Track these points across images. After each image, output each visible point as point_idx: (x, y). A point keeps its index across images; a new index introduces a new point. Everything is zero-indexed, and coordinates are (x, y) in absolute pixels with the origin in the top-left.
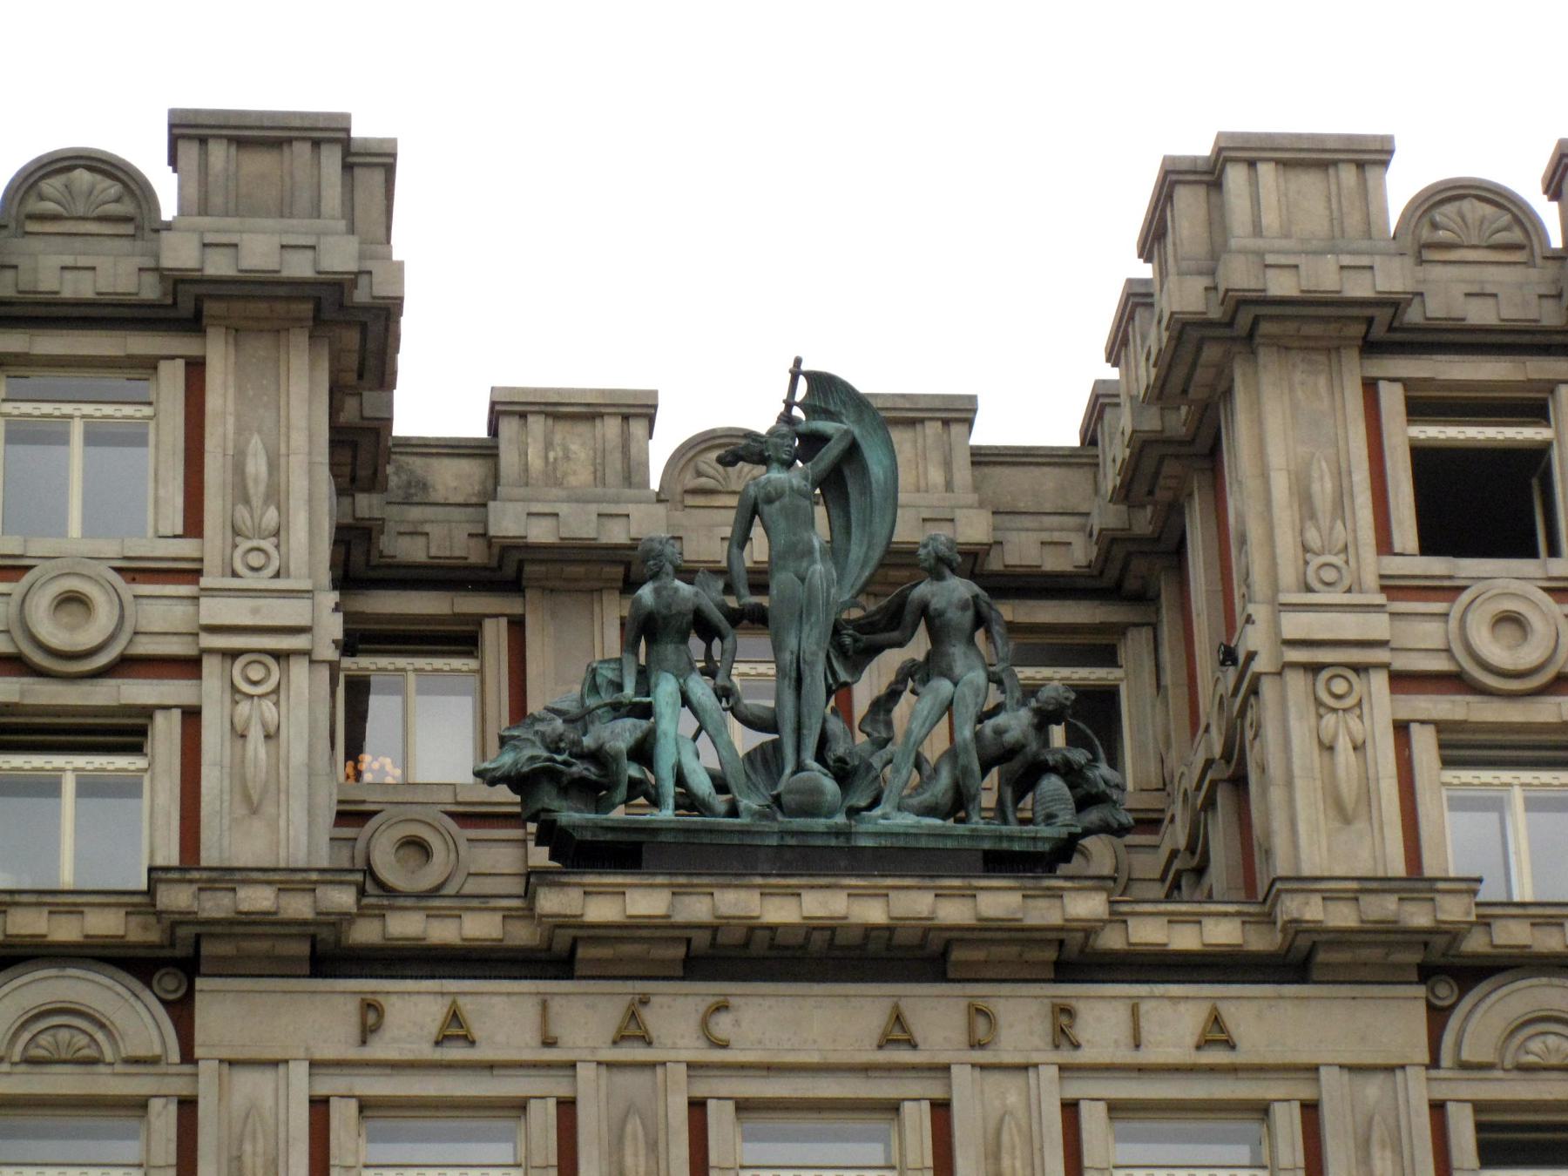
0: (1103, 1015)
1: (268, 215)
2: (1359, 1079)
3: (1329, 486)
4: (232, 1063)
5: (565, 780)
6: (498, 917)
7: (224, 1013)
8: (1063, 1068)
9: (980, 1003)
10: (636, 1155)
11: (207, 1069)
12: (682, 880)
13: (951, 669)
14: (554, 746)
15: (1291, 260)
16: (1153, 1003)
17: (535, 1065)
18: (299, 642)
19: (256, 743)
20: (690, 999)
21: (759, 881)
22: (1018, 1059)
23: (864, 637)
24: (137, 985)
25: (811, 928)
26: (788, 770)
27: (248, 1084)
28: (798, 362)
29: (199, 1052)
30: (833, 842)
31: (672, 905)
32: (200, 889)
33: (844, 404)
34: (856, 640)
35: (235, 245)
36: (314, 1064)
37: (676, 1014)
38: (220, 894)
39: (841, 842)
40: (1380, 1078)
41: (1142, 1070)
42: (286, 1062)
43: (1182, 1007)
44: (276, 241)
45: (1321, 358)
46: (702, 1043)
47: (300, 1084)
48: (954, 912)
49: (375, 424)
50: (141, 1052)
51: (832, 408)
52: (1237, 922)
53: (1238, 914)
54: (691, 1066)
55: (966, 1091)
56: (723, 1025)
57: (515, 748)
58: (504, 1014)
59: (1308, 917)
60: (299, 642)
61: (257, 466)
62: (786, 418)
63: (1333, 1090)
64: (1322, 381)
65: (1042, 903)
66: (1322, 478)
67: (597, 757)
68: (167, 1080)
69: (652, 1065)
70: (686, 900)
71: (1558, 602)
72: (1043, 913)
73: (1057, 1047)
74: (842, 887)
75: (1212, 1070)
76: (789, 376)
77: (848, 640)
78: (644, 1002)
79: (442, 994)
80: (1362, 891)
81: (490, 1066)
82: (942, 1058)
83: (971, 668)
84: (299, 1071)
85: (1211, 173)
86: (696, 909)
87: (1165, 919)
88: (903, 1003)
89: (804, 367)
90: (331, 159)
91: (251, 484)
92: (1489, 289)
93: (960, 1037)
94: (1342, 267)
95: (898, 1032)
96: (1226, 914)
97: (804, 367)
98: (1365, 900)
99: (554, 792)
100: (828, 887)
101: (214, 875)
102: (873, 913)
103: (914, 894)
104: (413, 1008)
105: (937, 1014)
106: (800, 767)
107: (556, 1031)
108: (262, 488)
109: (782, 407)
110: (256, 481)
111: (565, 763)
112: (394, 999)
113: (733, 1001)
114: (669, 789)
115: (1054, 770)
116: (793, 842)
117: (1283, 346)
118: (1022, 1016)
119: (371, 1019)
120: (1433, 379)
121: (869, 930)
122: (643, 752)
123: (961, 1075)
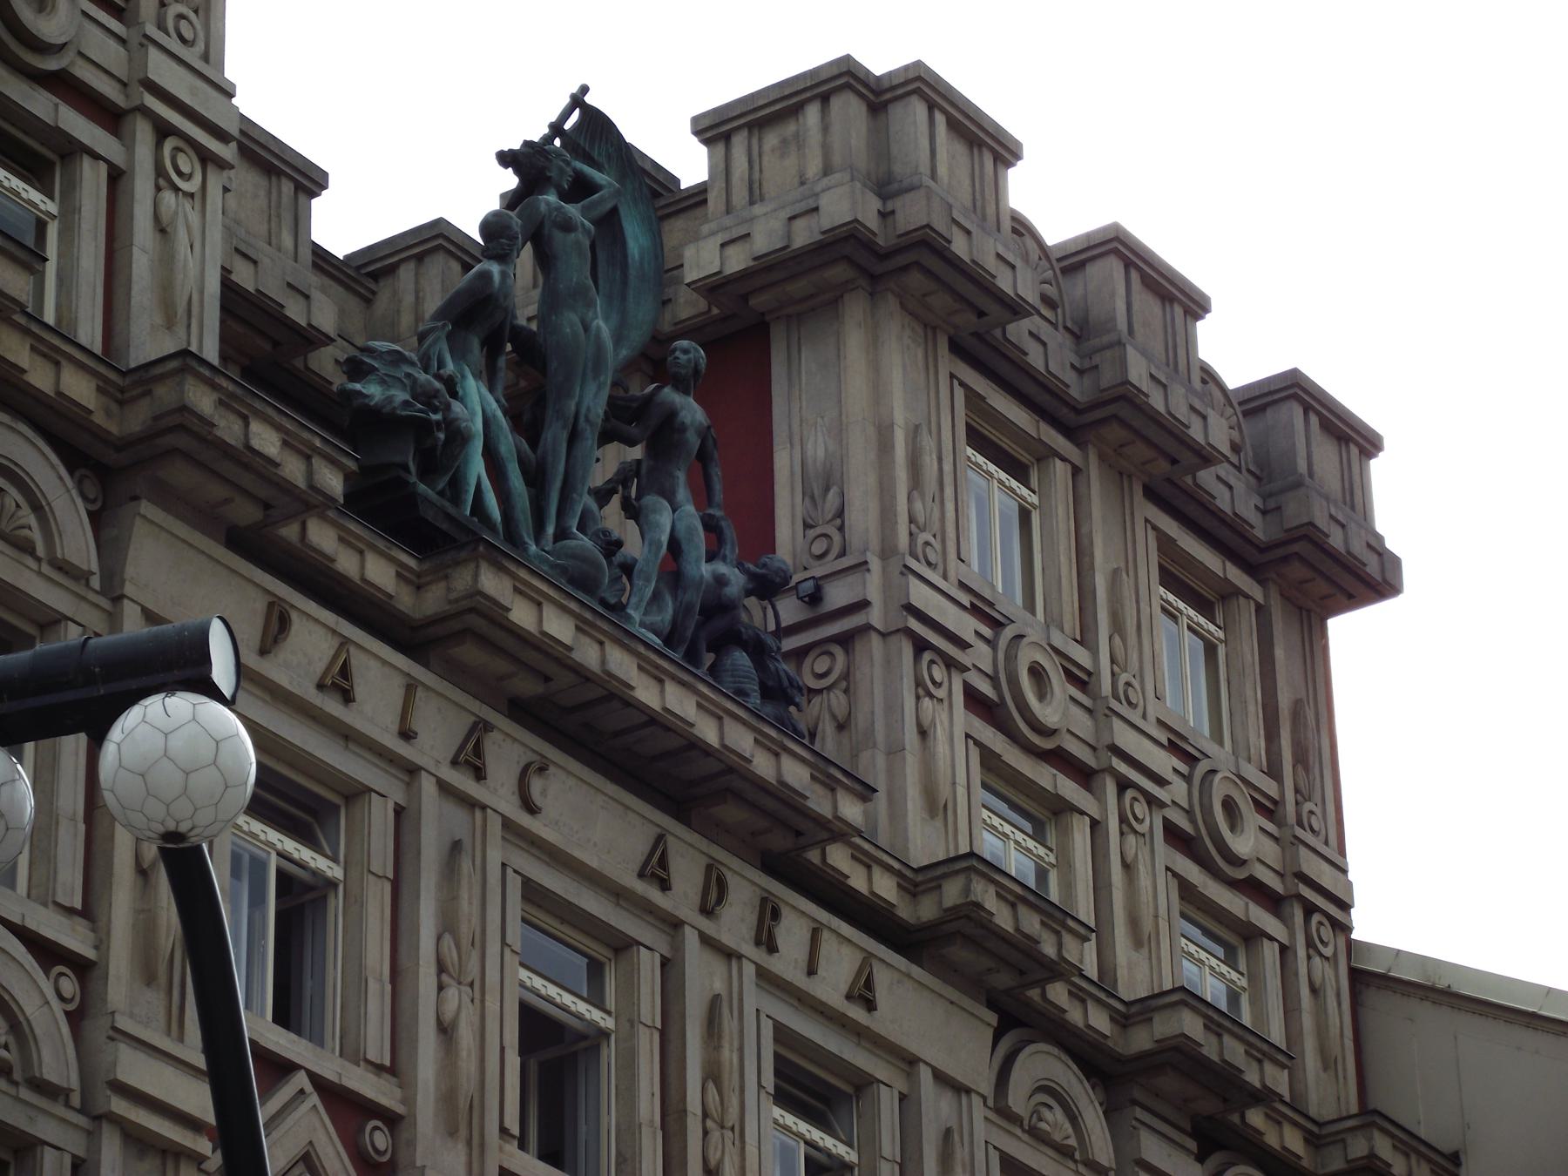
20: (516, 745)
25: (654, 721)
28: (584, 89)
33: (609, 157)
46: (515, 799)
51: (595, 155)
57: (382, 382)
62: (548, 139)
68: (84, 606)
76: (566, 100)
79: (334, 632)
81: (348, 736)
85: (877, 93)
86: (588, 654)
89: (588, 99)
95: (657, 870)
107: (416, 725)
115: (744, 645)
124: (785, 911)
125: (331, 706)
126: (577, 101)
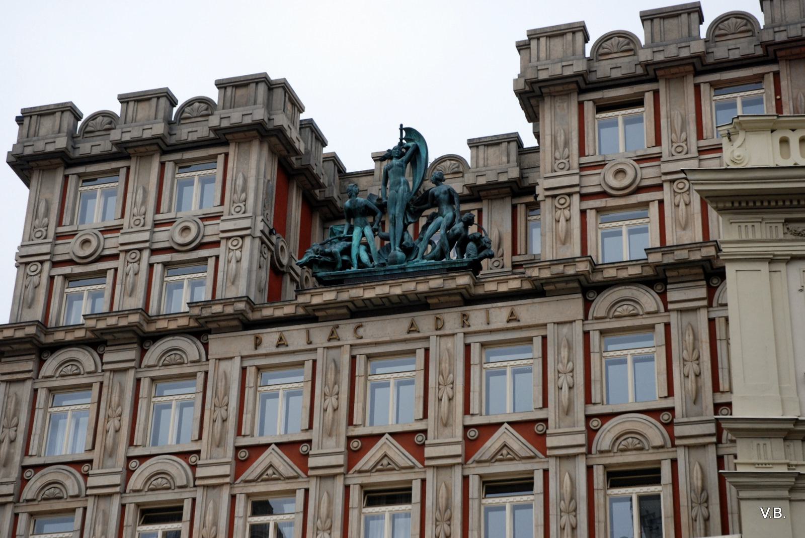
0: (477, 316)
1: (243, 106)
2: (560, 327)
3: (563, 137)
4: (220, 359)
5: (319, 263)
6: (294, 307)
7: (218, 345)
8: (465, 334)
9: (438, 316)
10: (331, 375)
11: (212, 362)
12: (339, 288)
13: (442, 213)
14: (316, 252)
15: (546, 67)
16: (493, 309)
17: (306, 350)
18: (248, 232)
19: (233, 264)
21: (362, 285)
22: (450, 332)
23: (417, 207)
24: (195, 339)
26: (392, 251)
27: (224, 365)
28: (401, 125)
29: (209, 357)
30: (400, 272)
31: (337, 296)
32: (202, 308)
34: (414, 208)
35: (229, 117)
36: (242, 357)
37: (346, 331)
38: (207, 309)
39: (403, 271)
40: (568, 325)
41: (491, 331)
42: (234, 357)
43: (503, 310)
44: (241, 113)
45: (566, 97)
47: (237, 364)
48: (422, 288)
49: (306, 167)
50: (194, 359)
51: (412, 138)
52: (520, 280)
53: (519, 278)
54: (351, 346)
55: (433, 344)
56: (361, 331)
58: (296, 336)
59: (533, 275)
60: (248, 232)
61: (240, 182)
63: (550, 331)
64: (565, 105)
65: (450, 281)
66: (561, 135)
67: (331, 254)
68: (203, 366)
69: (340, 347)
70: (342, 294)
71: (638, 164)
72: (451, 284)
73: (463, 327)
74: (387, 284)
75: (514, 329)
76: (399, 131)
77: (411, 209)
78: (337, 327)
80: (550, 265)
82: (427, 334)
83: (448, 212)
84: (237, 360)
86: (345, 296)
87: (496, 282)
88: (415, 319)
89: (404, 127)
90: (262, 88)
91: (237, 187)
92: (619, 65)
93: (432, 327)
94: (563, 66)
95: (413, 328)
96: (516, 278)
97: (404, 127)
98: (553, 267)
99: (317, 267)
100: (383, 284)
101: (205, 303)
102: (397, 291)
103: (409, 284)
104: (270, 337)
105: (425, 321)
106: (395, 250)
107: (311, 339)
108: (240, 188)
109: (399, 141)
110: (239, 186)
111: (319, 257)
112: (265, 335)
113: (363, 324)
114: (355, 261)
116: (388, 273)
117: (552, 96)
118: (451, 318)
119: (258, 343)
120: (603, 98)
121: (398, 296)
122: (347, 251)
123: (433, 339)
124: (468, 313)
125: (282, 349)
126: (401, 129)
